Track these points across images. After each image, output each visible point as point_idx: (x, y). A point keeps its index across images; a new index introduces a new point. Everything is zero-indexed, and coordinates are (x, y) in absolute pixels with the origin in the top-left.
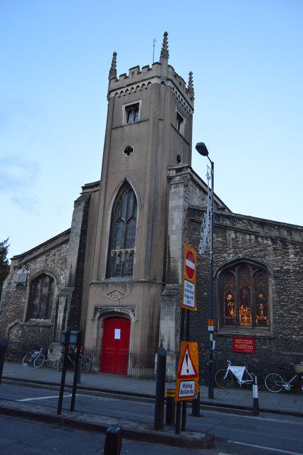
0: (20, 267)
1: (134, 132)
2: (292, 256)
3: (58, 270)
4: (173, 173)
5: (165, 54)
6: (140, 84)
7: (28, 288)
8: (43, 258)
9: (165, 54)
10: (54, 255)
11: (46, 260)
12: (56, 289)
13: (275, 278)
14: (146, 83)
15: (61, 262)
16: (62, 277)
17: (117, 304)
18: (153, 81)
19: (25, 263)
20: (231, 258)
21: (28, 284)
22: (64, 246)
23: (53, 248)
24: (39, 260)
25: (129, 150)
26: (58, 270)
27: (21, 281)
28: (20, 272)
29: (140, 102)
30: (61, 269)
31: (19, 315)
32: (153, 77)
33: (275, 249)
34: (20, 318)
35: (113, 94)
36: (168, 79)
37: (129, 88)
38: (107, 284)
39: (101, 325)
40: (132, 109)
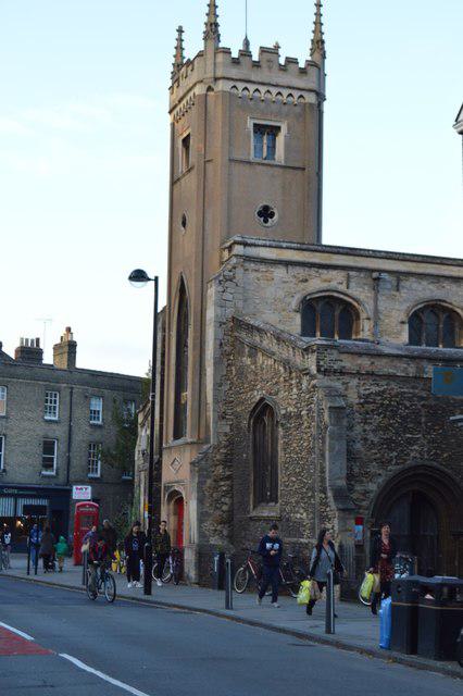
1: (190, 183)
2: (295, 390)
4: (226, 254)
5: (212, 30)
6: (188, 98)
9: (212, 30)
13: (282, 425)
14: (191, 94)
18: (199, 90)
20: (258, 398)
32: (195, 85)
33: (285, 381)
36: (216, 79)
37: (181, 105)
39: (171, 512)
40: (186, 141)
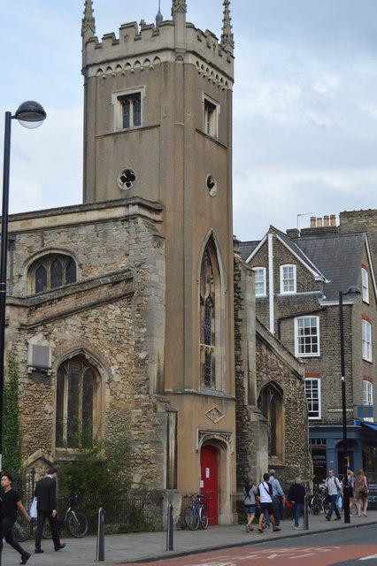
0: (32, 329)
3: (106, 352)
7: (54, 380)
8: (75, 321)
10: (97, 320)
11: (83, 328)
12: (108, 392)
15: (109, 337)
16: (113, 369)
17: (216, 428)
19: (44, 322)
21: (55, 370)
22: (110, 306)
23: (93, 306)
24: (69, 321)
25: (210, 186)
26: (106, 352)
27: (40, 363)
28: (35, 340)
29: (218, 107)
30: (111, 352)
31: (42, 438)
34: (46, 446)
35: (191, 59)
37: (211, 69)
38: (206, 396)
